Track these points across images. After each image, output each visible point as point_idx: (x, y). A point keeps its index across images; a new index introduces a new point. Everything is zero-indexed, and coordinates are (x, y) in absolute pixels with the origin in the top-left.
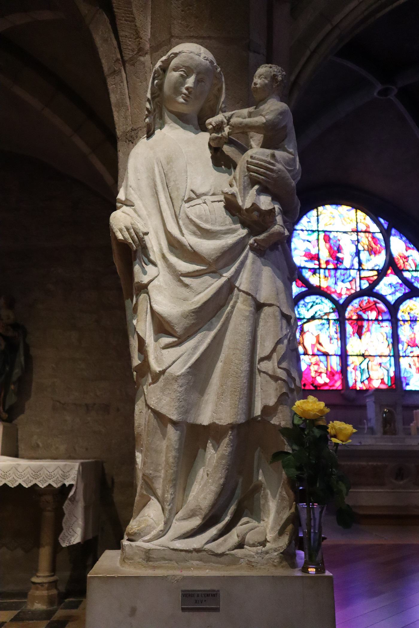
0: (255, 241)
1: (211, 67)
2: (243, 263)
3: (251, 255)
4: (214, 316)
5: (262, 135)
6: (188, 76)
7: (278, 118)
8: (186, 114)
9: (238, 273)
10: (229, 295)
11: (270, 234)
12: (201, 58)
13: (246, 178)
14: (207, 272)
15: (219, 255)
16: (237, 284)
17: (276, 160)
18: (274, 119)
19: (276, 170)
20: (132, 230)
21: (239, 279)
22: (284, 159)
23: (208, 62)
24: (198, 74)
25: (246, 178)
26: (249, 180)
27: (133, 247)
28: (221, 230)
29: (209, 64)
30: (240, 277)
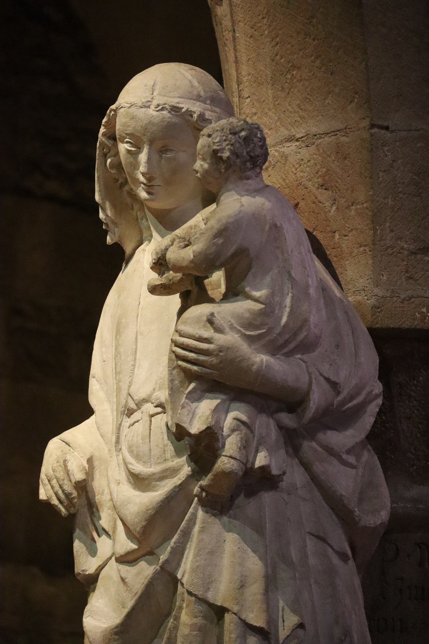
0: (202, 488)
1: (175, 120)
2: (187, 535)
3: (200, 513)
4: (155, 637)
5: (178, 295)
6: (139, 149)
7: (214, 244)
8: (169, 211)
9: (178, 553)
10: (173, 597)
11: (216, 475)
12: (152, 111)
13: (175, 372)
14: (139, 554)
15: (144, 523)
16: (179, 576)
17: (218, 330)
18: (206, 250)
19: (214, 350)
20: (54, 482)
21: (182, 565)
22: (239, 317)
23: (165, 112)
24: (151, 143)
25: (175, 372)
26: (182, 374)
27: (60, 511)
28: (154, 474)
29: (169, 115)
30: (184, 560)
